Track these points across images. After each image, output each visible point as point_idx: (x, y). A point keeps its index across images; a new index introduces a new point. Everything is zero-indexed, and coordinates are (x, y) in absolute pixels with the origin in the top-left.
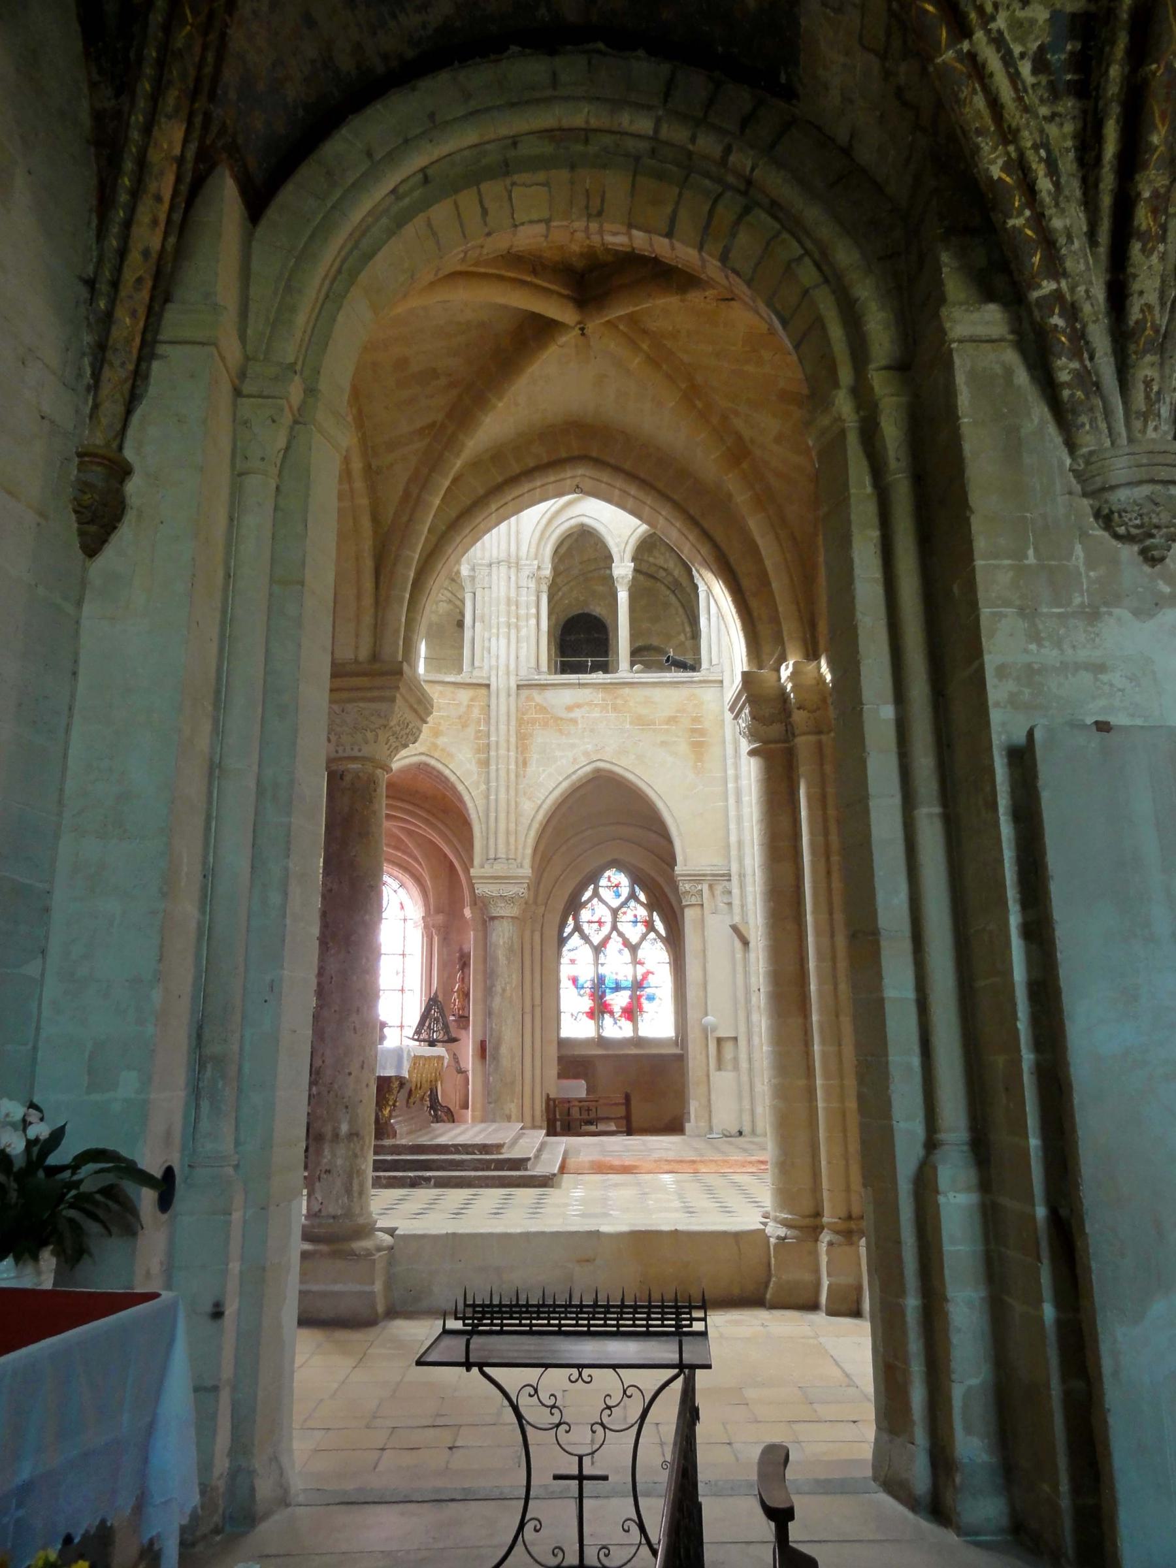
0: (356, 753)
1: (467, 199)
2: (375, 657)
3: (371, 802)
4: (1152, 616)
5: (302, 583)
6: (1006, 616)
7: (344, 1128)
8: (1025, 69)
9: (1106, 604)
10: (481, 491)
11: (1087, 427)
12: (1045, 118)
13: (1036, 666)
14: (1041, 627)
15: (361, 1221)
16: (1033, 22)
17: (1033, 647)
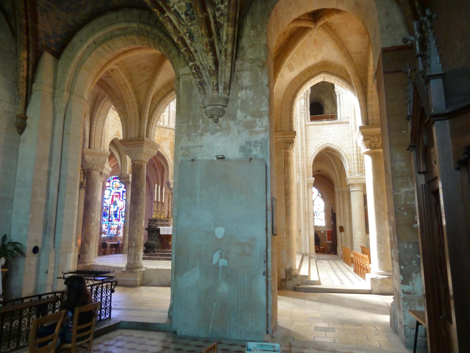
0: (137, 159)
1: (104, 45)
2: (139, 136)
3: (141, 170)
4: (214, 134)
5: (70, 134)
6: (184, 136)
7: (134, 245)
8: (183, 16)
9: (205, 132)
10: (165, 93)
11: (202, 93)
12: (190, 26)
13: (189, 147)
14: (191, 138)
15: (138, 265)
16: (182, 6)
17: (189, 143)
